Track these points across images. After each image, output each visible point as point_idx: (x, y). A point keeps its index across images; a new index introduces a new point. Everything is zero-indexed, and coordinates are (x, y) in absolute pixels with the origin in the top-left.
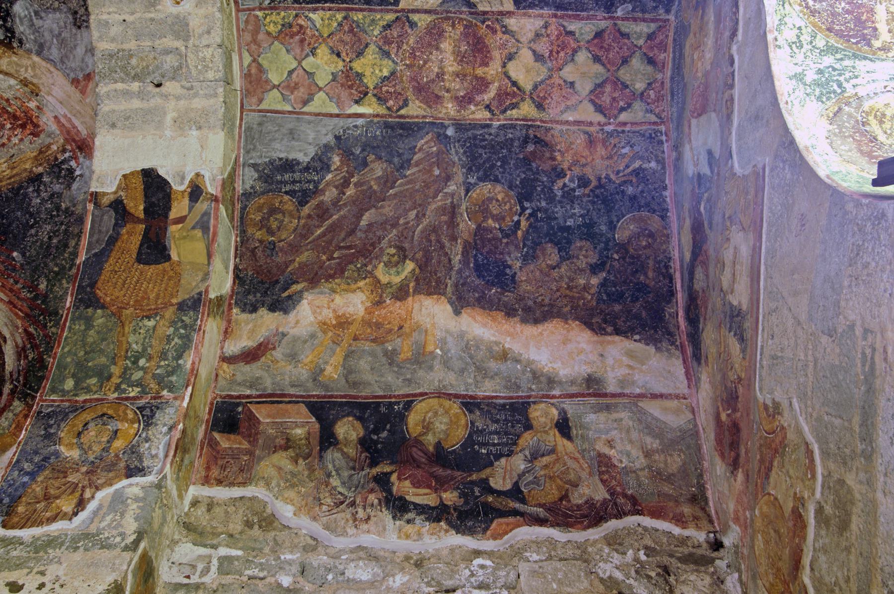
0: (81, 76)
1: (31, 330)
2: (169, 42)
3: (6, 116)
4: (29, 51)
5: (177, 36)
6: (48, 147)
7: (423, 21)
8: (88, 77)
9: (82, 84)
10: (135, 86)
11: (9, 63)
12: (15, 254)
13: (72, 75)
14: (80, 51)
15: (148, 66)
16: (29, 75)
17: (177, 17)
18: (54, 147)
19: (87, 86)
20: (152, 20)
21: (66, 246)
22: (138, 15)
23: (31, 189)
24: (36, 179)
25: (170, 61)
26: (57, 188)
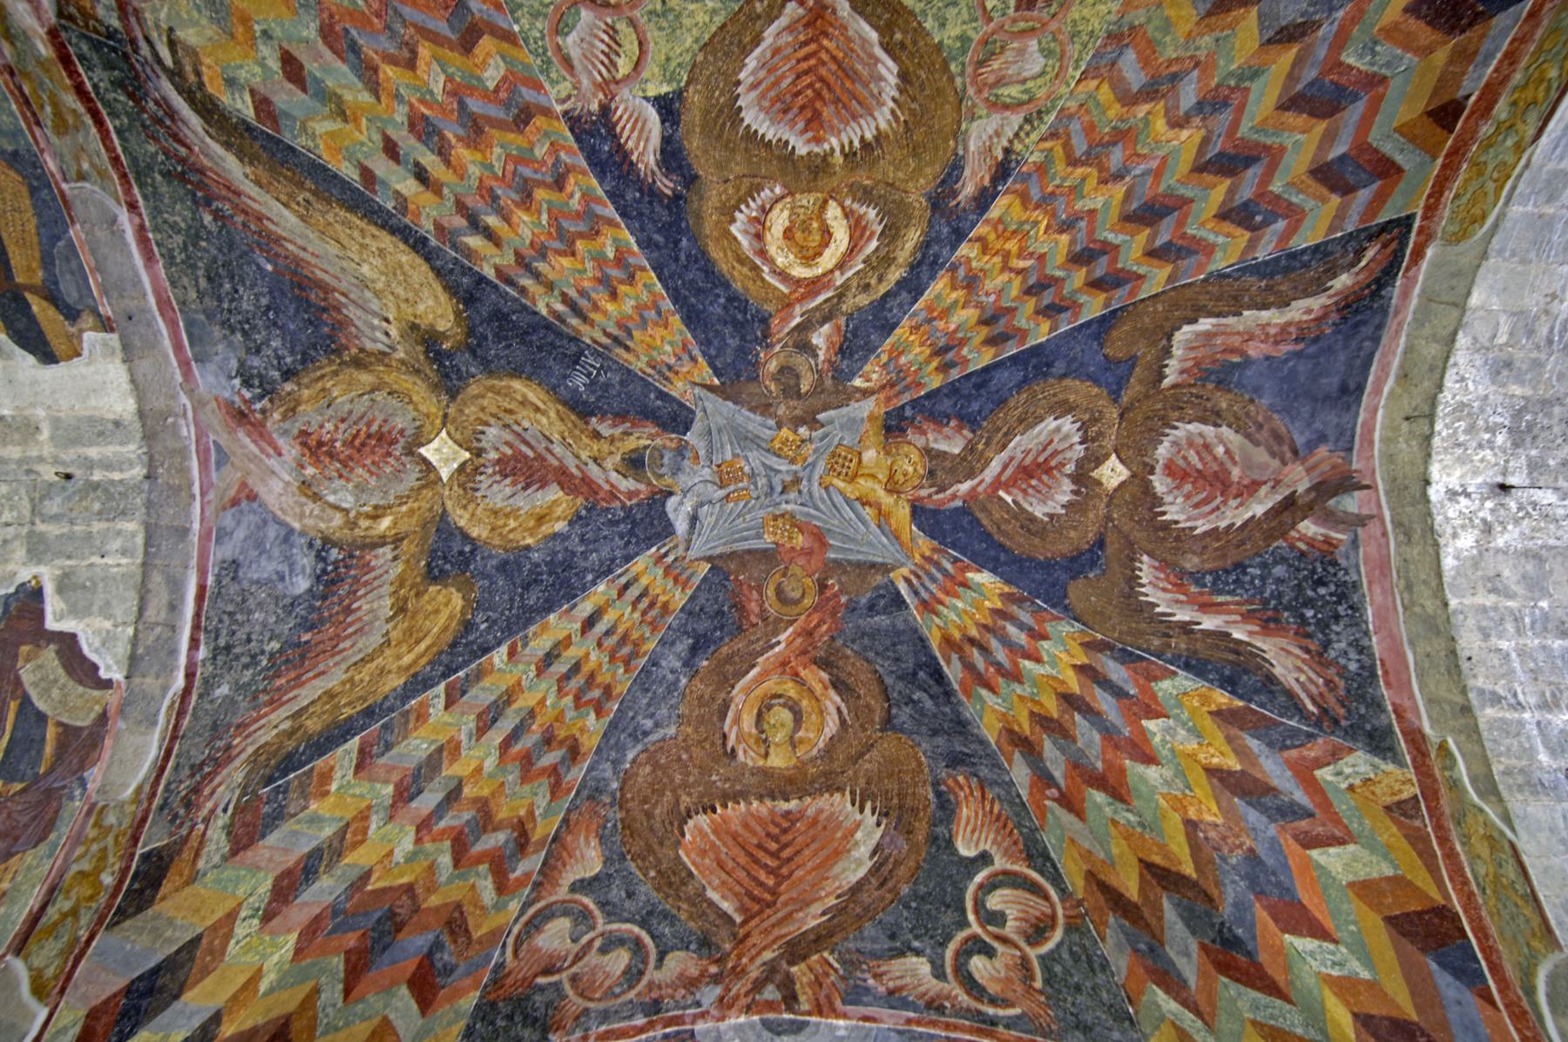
0: (244, 504)
1: (183, 151)
2: (52, 530)
3: (342, 456)
4: (302, 534)
5: (42, 538)
6: (285, 418)
8: (235, 502)
9: (243, 495)
10: (97, 476)
11: (330, 520)
12: (269, 268)
13: (255, 505)
14: (240, 534)
15: (81, 499)
16: (310, 506)
17: (39, 562)
18: (277, 416)
19: (238, 492)
20: (69, 557)
21: (209, 279)
22: (85, 563)
23: (289, 360)
24: (288, 374)
25: (53, 506)
26: (256, 362)
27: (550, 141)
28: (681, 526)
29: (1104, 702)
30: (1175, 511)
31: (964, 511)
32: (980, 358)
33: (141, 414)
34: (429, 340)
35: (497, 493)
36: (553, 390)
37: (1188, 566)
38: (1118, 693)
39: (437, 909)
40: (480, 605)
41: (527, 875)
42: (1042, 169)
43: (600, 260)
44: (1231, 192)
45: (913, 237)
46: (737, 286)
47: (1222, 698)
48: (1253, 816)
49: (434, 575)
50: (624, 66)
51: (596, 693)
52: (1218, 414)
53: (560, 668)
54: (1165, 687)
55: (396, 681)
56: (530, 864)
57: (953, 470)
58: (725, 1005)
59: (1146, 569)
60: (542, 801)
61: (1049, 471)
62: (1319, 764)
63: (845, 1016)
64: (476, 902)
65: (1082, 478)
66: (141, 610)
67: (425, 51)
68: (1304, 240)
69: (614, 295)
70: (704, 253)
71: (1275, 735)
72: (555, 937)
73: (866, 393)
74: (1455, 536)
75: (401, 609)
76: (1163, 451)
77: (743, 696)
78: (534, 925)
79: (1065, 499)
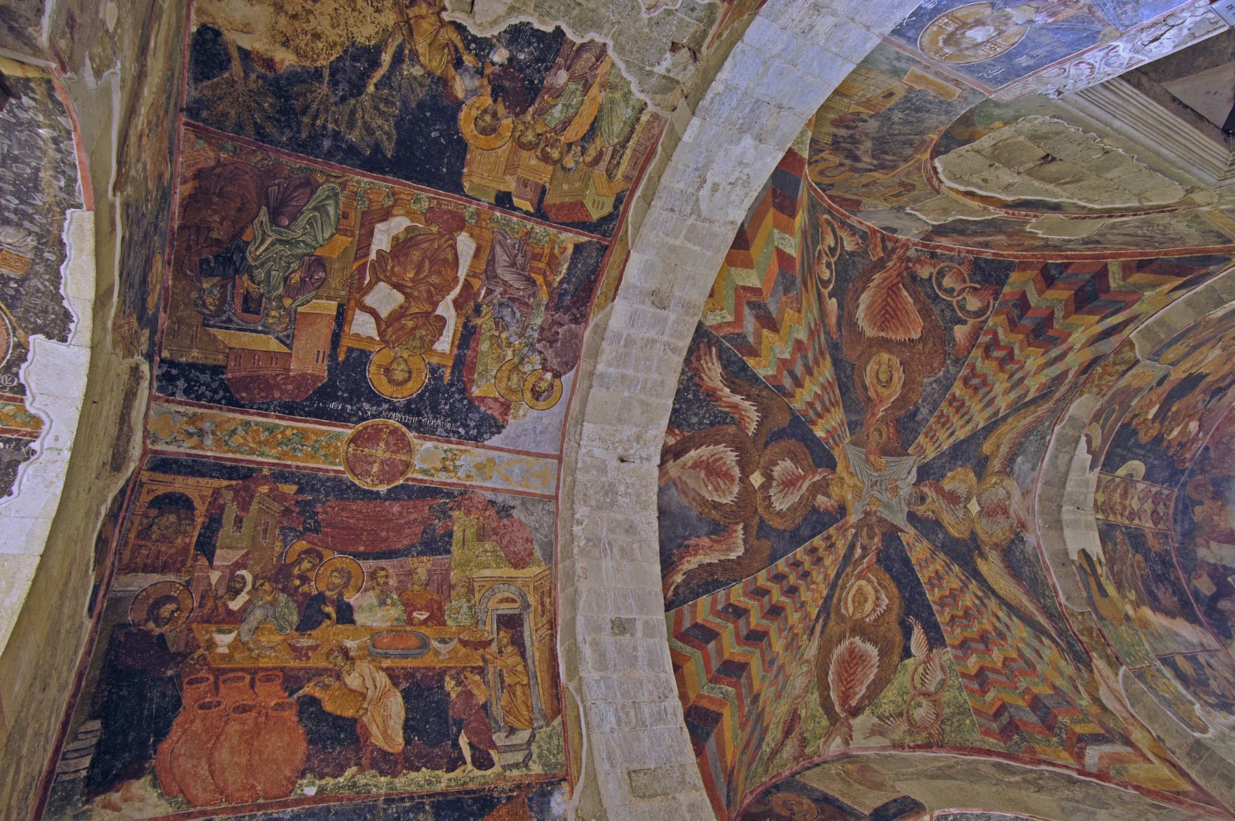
7: (1117, 480)
27: (953, 635)
28: (914, 470)
29: (799, 369)
30: (731, 457)
31: (818, 466)
32: (817, 541)
33: (1062, 529)
34: (983, 555)
35: (962, 490)
36: (947, 533)
37: (734, 428)
38: (792, 373)
39: (1019, 332)
40: (980, 445)
41: (985, 335)
42: (804, 633)
43: (940, 586)
44: (748, 623)
45: (835, 600)
46: (888, 576)
47: (751, 362)
48: (772, 308)
49: (987, 458)
50: (921, 670)
51: (955, 404)
52: (715, 508)
53: (966, 417)
54: (771, 372)
55: (1010, 420)
56: (984, 339)
57: (821, 486)
58: (906, 246)
59: (752, 428)
60: (979, 363)
61: (783, 483)
62: (729, 324)
63: (868, 227)
64: (1005, 330)
65: (769, 477)
66: (1072, 458)
67: (1000, 665)
68: (704, 601)
69: (937, 572)
70: (900, 591)
71: (739, 341)
72: (973, 304)
73: (852, 526)
74: (656, 437)
75: (999, 447)
76: (736, 489)
77: (896, 390)
78: (981, 313)
79: (777, 468)
